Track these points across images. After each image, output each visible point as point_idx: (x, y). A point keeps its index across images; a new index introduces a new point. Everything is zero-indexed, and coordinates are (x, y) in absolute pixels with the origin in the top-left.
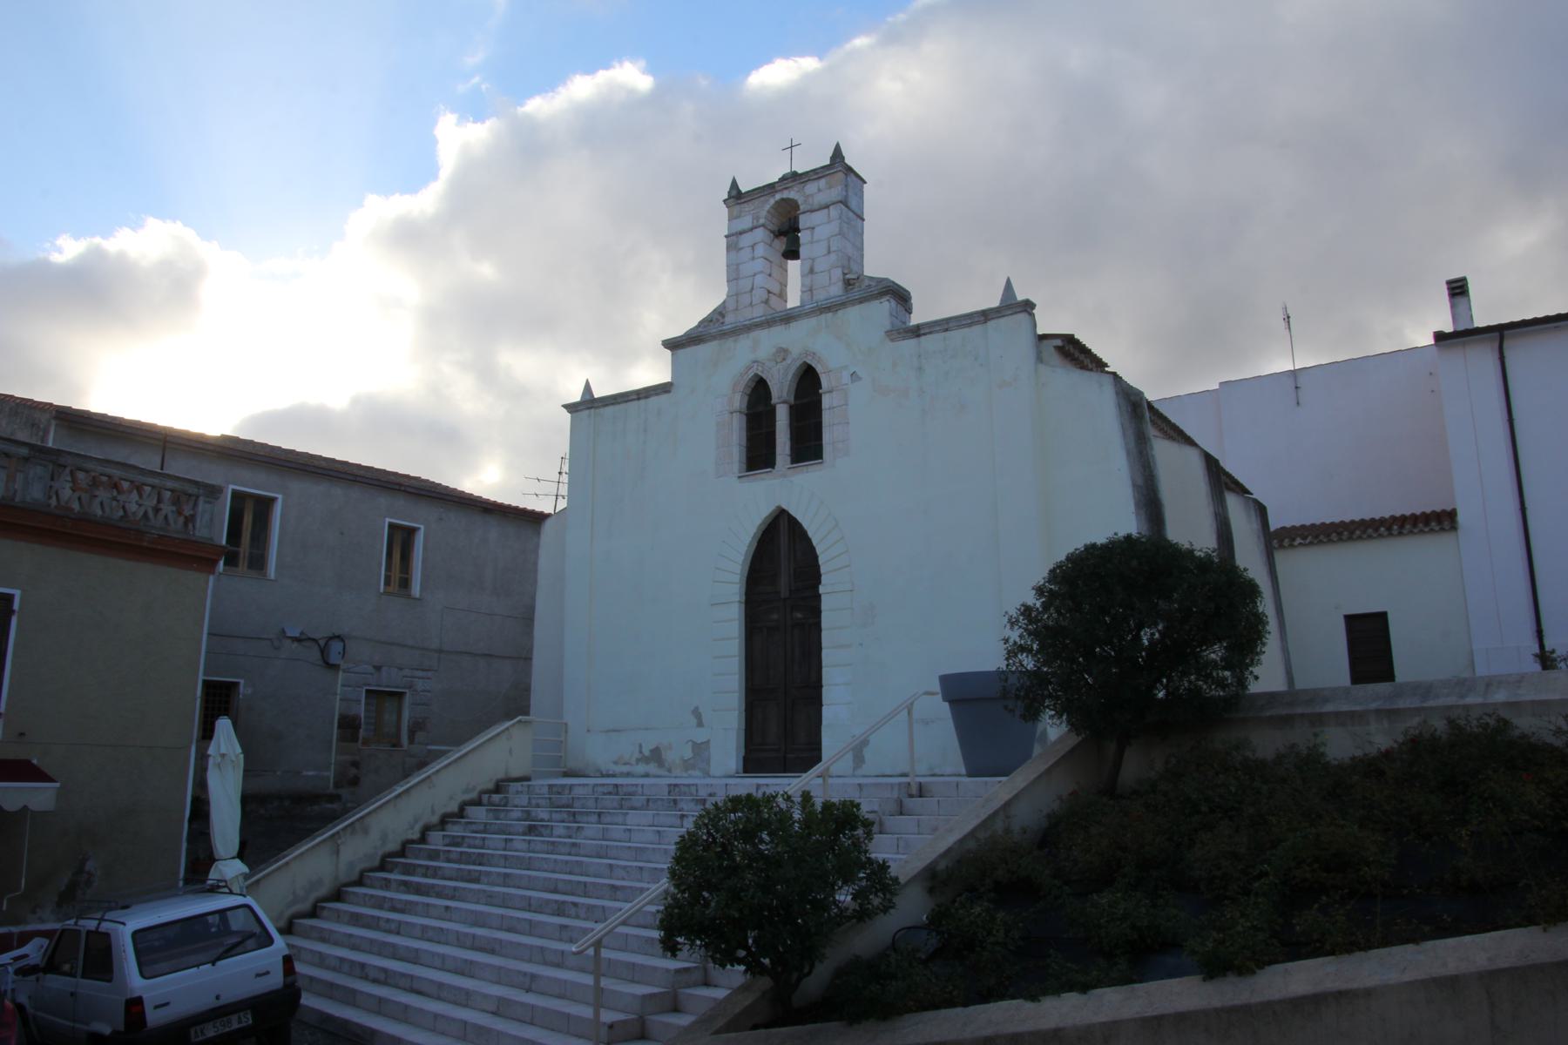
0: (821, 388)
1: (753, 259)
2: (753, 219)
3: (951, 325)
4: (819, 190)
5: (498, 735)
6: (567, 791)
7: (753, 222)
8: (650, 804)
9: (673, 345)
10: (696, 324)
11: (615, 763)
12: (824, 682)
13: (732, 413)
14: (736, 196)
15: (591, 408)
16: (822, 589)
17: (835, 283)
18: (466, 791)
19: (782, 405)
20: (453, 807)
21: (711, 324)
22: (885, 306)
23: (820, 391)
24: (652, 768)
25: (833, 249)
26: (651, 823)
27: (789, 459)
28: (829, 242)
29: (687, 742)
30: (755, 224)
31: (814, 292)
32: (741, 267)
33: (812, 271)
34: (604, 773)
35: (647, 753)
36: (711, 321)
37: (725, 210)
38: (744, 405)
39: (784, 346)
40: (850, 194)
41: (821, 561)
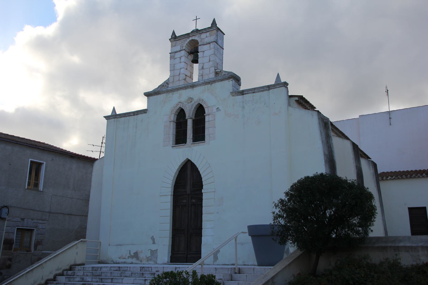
0: (205, 114)
1: (180, 62)
2: (181, 47)
3: (255, 91)
4: (207, 37)
5: (72, 246)
6: (99, 270)
8: (133, 275)
9: (148, 95)
11: (120, 258)
12: (203, 227)
13: (170, 122)
14: (174, 38)
15: (115, 118)
16: (203, 191)
17: (211, 73)
18: (58, 270)
19: (190, 119)
20: (51, 277)
21: (163, 87)
22: (230, 83)
23: (205, 114)
24: (134, 260)
25: (211, 60)
26: (133, 283)
27: (192, 140)
29: (149, 250)
30: (181, 49)
31: (203, 76)
32: (175, 65)
33: (203, 68)
34: (115, 262)
35: (132, 254)
36: (163, 86)
38: (175, 119)
39: (191, 97)
40: (218, 39)
41: (203, 180)
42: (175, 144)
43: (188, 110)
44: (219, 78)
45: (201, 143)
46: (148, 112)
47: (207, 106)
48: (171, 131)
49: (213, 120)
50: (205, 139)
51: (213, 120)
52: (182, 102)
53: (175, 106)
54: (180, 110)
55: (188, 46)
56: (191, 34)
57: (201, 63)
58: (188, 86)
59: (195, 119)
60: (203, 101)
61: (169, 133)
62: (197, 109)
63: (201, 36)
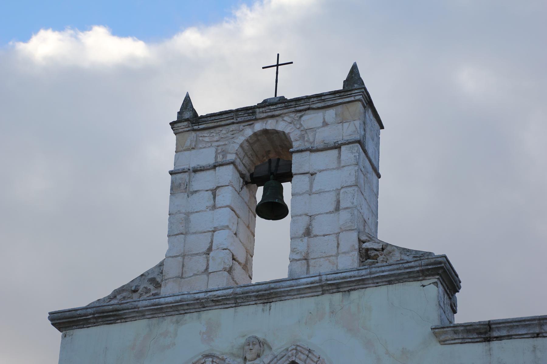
1: (214, 207)
2: (217, 153)
7: (216, 157)
10: (108, 292)
17: (344, 253)
21: (135, 296)
25: (343, 205)
28: (339, 194)
31: (312, 262)
32: (192, 217)
33: (308, 233)
36: (135, 291)
37: (171, 138)
39: (260, 336)
40: (368, 136)
44: (383, 268)
52: (217, 354)
55: (246, 154)
56: (264, 109)
57: (301, 215)
58: (247, 293)
60: (310, 355)
63: (303, 118)
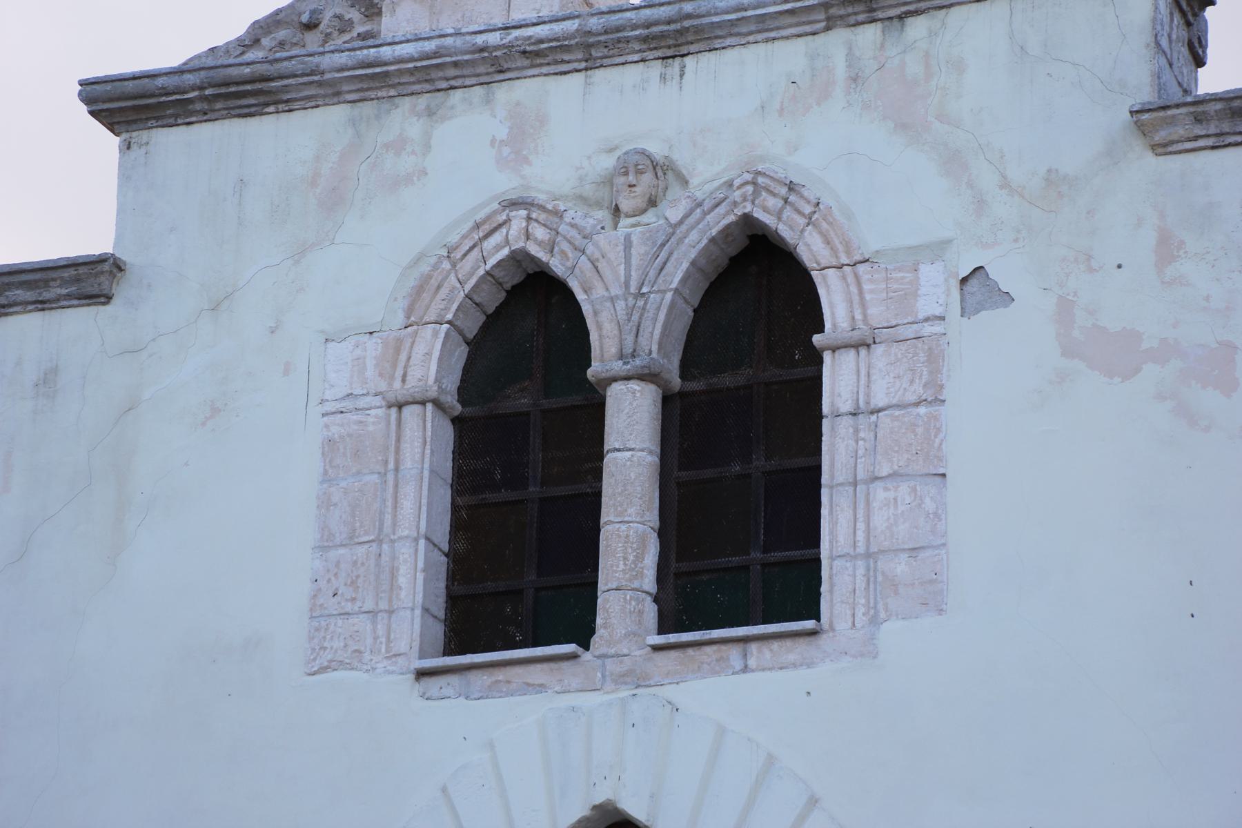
0: (820, 328)
19: (635, 386)
23: (817, 339)
36: (310, 26)
38: (452, 382)
39: (656, 149)
42: (448, 652)
43: (616, 290)
45: (776, 645)
46: (123, 291)
47: (848, 253)
48: (408, 505)
49: (917, 404)
50: (817, 595)
51: (912, 398)
52: (541, 198)
53: (454, 238)
54: (508, 286)
58: (618, 29)
59: (682, 394)
60: (792, 198)
61: (388, 518)
62: (712, 284)
